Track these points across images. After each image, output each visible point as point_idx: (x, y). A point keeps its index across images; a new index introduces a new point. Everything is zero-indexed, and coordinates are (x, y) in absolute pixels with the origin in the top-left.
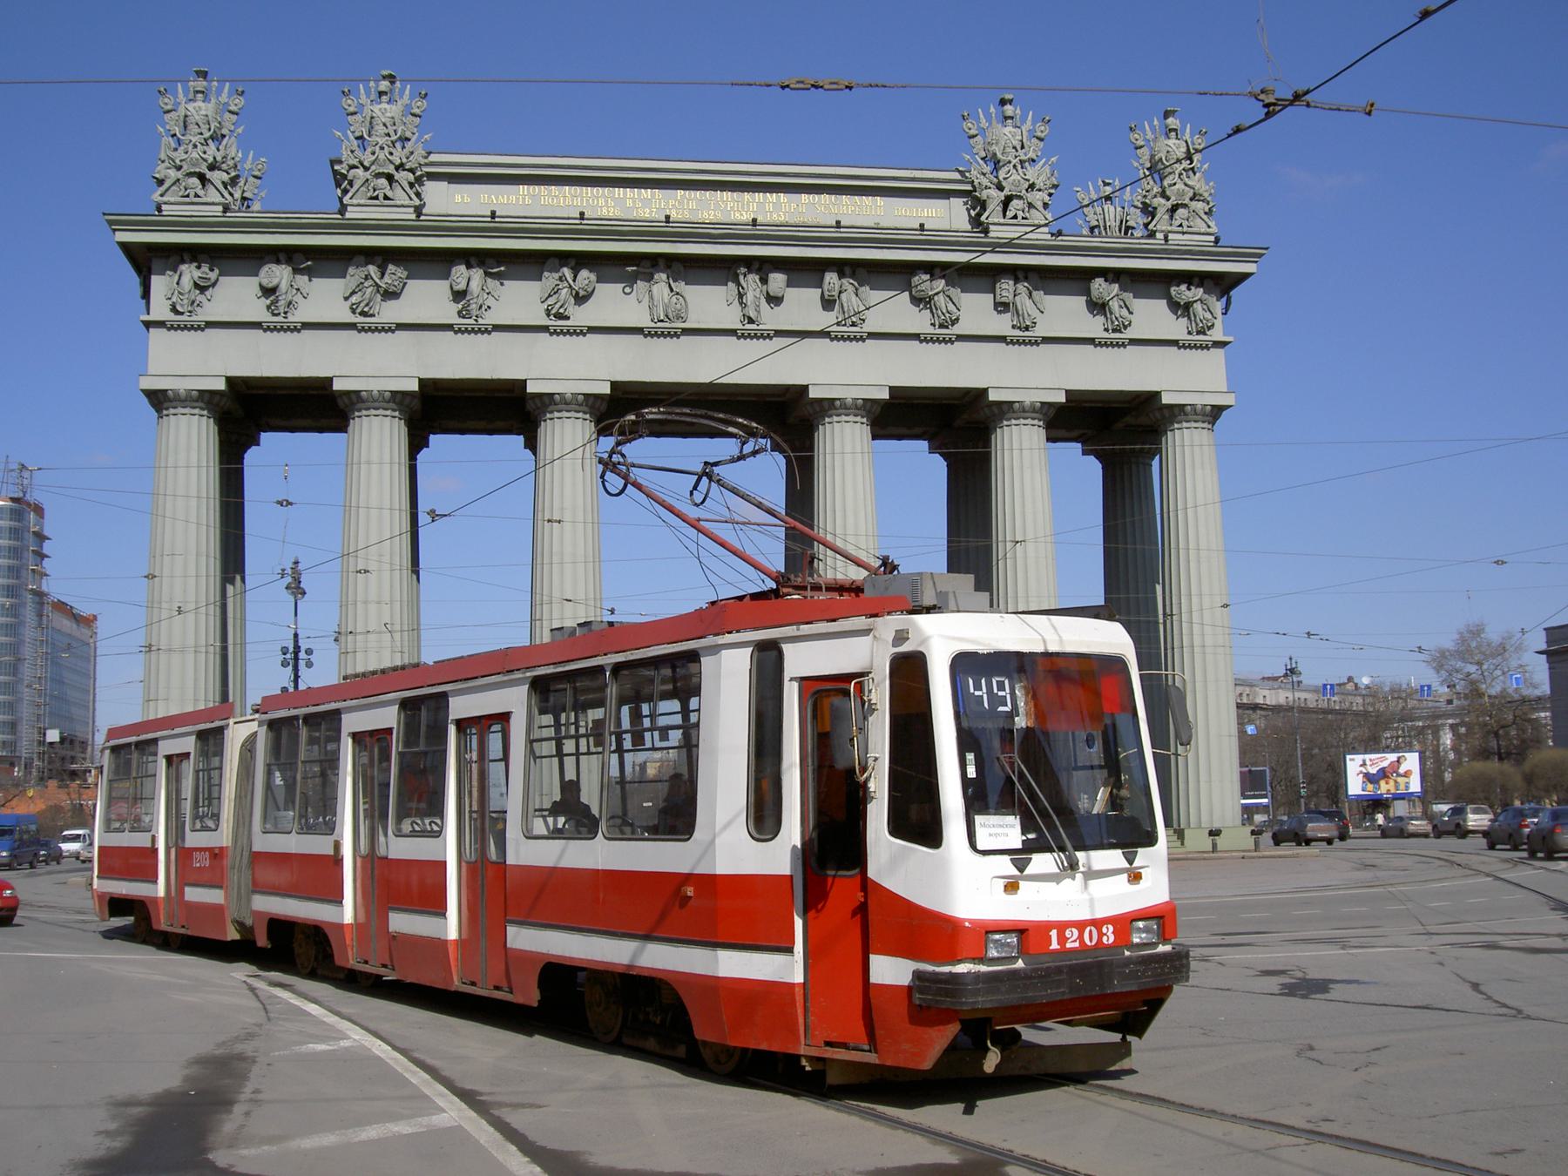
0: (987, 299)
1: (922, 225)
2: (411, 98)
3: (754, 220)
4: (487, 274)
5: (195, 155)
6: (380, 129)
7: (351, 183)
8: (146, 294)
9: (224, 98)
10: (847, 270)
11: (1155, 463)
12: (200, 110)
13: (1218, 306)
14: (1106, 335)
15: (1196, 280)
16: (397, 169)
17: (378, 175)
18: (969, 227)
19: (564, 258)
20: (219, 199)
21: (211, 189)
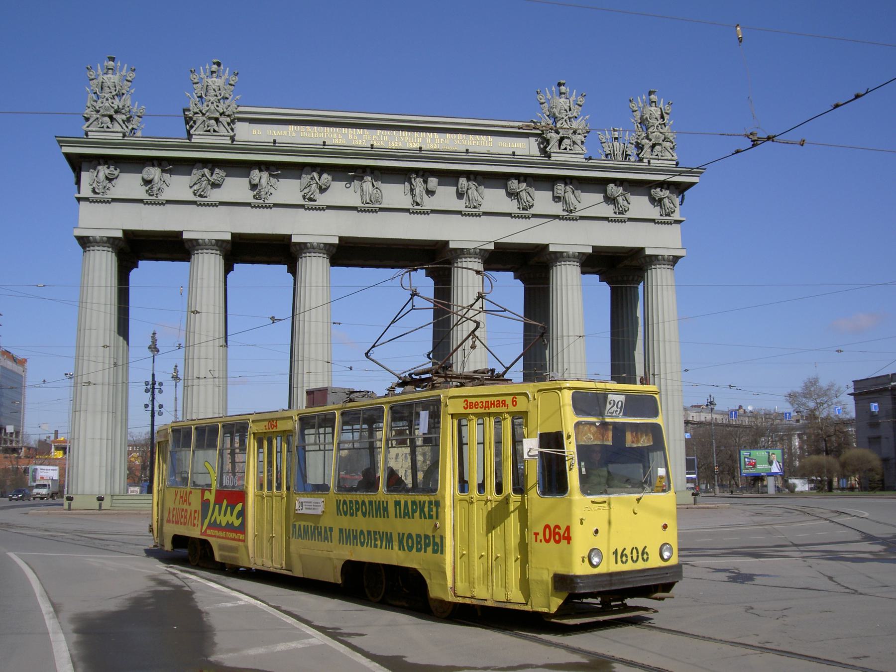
0: (549, 194)
1: (514, 153)
2: (229, 75)
3: (421, 148)
4: (270, 175)
5: (107, 104)
6: (212, 92)
7: (195, 122)
8: (78, 182)
9: (124, 73)
10: (472, 177)
11: (641, 287)
12: (111, 79)
13: (677, 201)
14: (615, 216)
15: (665, 186)
16: (221, 114)
17: (210, 118)
18: (539, 154)
19: (314, 167)
20: (120, 129)
21: (116, 124)
